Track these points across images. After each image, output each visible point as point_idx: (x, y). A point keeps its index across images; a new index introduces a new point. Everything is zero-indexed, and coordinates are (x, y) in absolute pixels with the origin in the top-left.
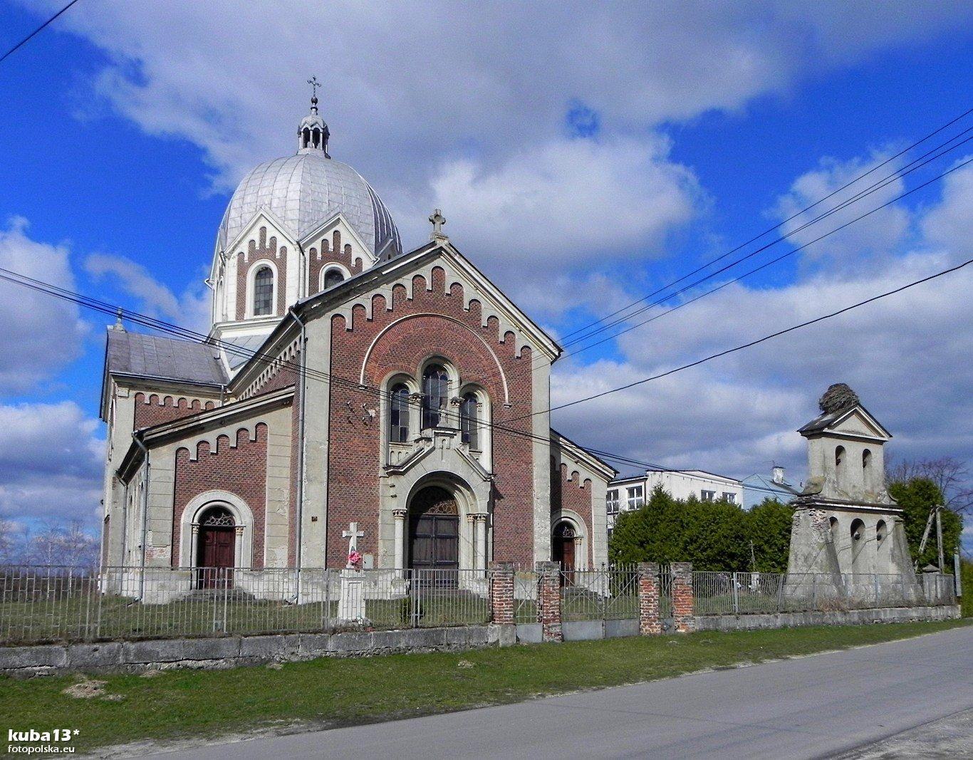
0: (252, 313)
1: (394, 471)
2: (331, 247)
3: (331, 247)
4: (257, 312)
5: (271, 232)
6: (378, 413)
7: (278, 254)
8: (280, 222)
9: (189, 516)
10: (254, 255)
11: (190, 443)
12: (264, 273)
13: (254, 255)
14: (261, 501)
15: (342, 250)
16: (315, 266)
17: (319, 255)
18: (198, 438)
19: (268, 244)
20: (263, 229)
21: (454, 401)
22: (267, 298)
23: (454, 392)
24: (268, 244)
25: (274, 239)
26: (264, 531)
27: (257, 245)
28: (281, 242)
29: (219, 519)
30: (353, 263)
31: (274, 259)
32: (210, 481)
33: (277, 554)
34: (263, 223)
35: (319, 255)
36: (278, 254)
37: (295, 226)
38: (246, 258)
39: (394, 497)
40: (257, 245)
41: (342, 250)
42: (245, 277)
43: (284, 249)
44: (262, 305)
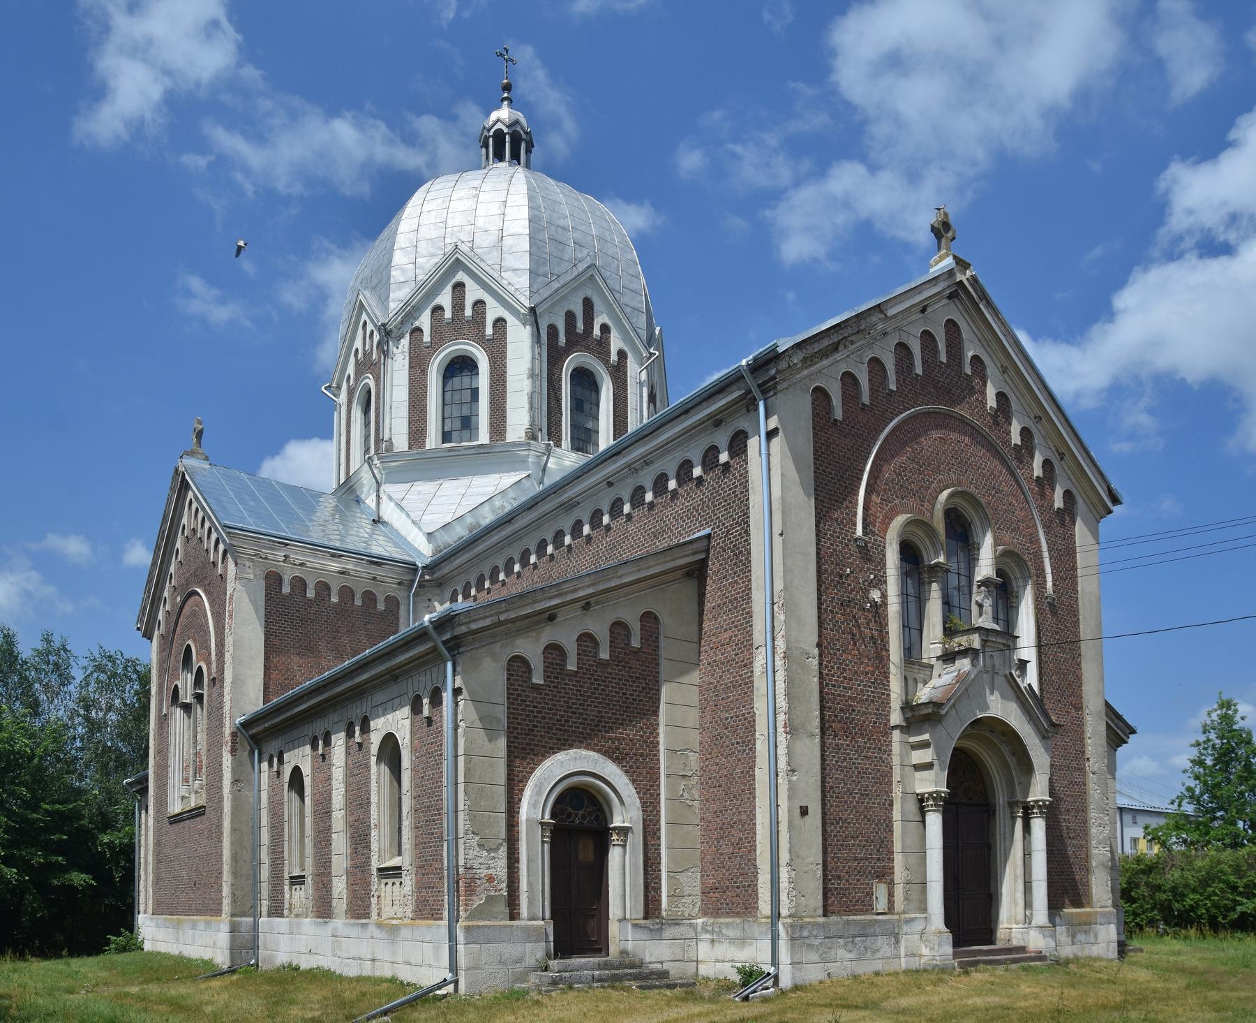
0: (440, 440)
1: (921, 717)
2: (580, 326)
3: (580, 326)
4: (446, 437)
5: (473, 292)
6: (884, 596)
7: (489, 331)
8: (496, 275)
9: (534, 805)
10: (442, 331)
11: (531, 648)
12: (461, 366)
13: (442, 331)
14: (654, 774)
15: (597, 331)
16: (555, 356)
17: (562, 339)
18: (548, 635)
19: (468, 312)
20: (459, 287)
21: (985, 583)
22: (466, 412)
23: (985, 567)
24: (468, 312)
25: (479, 304)
26: (659, 838)
27: (448, 314)
28: (494, 311)
29: (581, 813)
30: (614, 357)
31: (481, 340)
32: (566, 731)
33: (682, 885)
34: (461, 276)
35: (562, 339)
36: (489, 331)
37: (523, 281)
38: (427, 338)
39: (919, 772)
40: (448, 314)
41: (597, 331)
42: (424, 372)
43: (500, 323)
44: (457, 424)
